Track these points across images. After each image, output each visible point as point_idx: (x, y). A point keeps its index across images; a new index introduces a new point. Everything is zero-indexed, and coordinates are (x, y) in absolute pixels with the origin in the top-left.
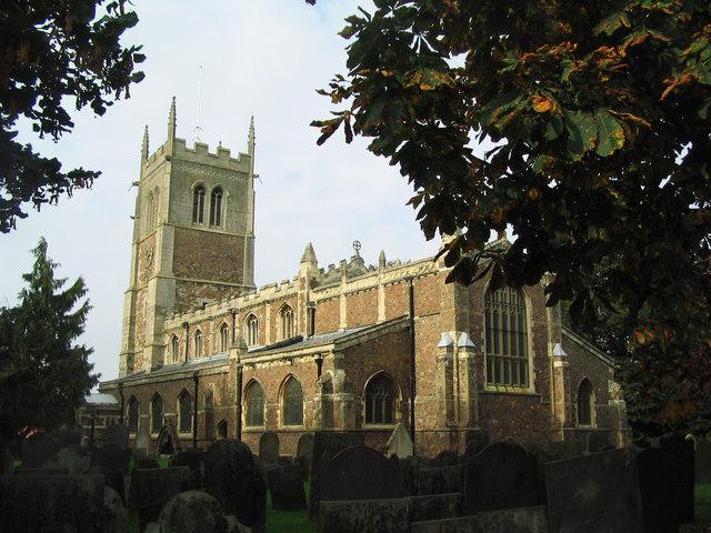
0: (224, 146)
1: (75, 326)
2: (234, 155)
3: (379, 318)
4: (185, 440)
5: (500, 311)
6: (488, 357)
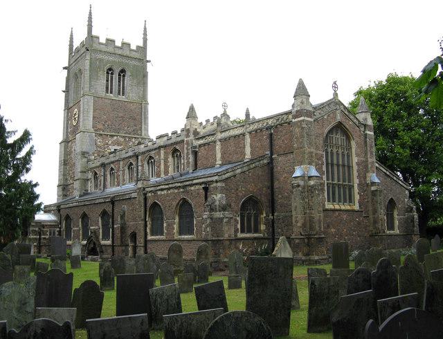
0: (125, 41)
1: (25, 164)
2: (133, 47)
3: (246, 157)
4: (105, 246)
5: (335, 150)
6: (327, 184)
